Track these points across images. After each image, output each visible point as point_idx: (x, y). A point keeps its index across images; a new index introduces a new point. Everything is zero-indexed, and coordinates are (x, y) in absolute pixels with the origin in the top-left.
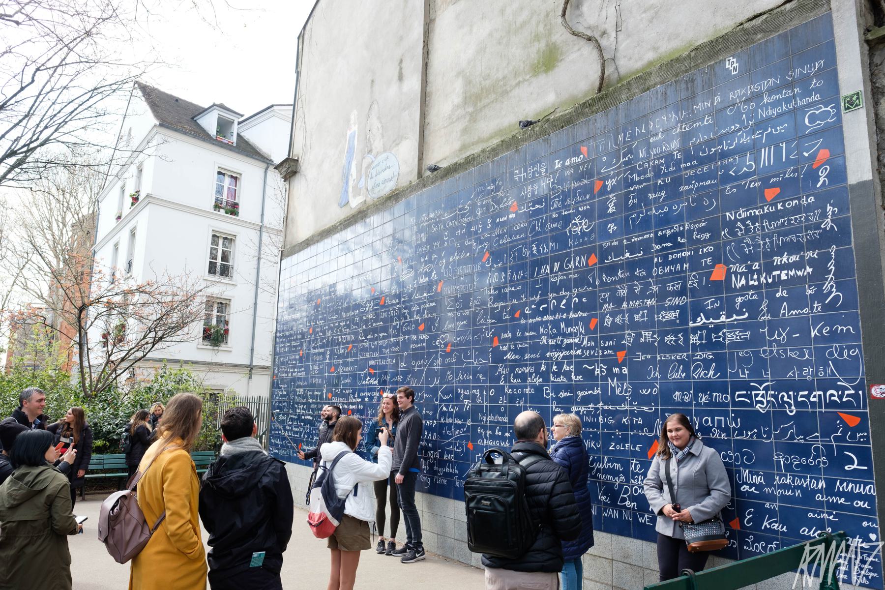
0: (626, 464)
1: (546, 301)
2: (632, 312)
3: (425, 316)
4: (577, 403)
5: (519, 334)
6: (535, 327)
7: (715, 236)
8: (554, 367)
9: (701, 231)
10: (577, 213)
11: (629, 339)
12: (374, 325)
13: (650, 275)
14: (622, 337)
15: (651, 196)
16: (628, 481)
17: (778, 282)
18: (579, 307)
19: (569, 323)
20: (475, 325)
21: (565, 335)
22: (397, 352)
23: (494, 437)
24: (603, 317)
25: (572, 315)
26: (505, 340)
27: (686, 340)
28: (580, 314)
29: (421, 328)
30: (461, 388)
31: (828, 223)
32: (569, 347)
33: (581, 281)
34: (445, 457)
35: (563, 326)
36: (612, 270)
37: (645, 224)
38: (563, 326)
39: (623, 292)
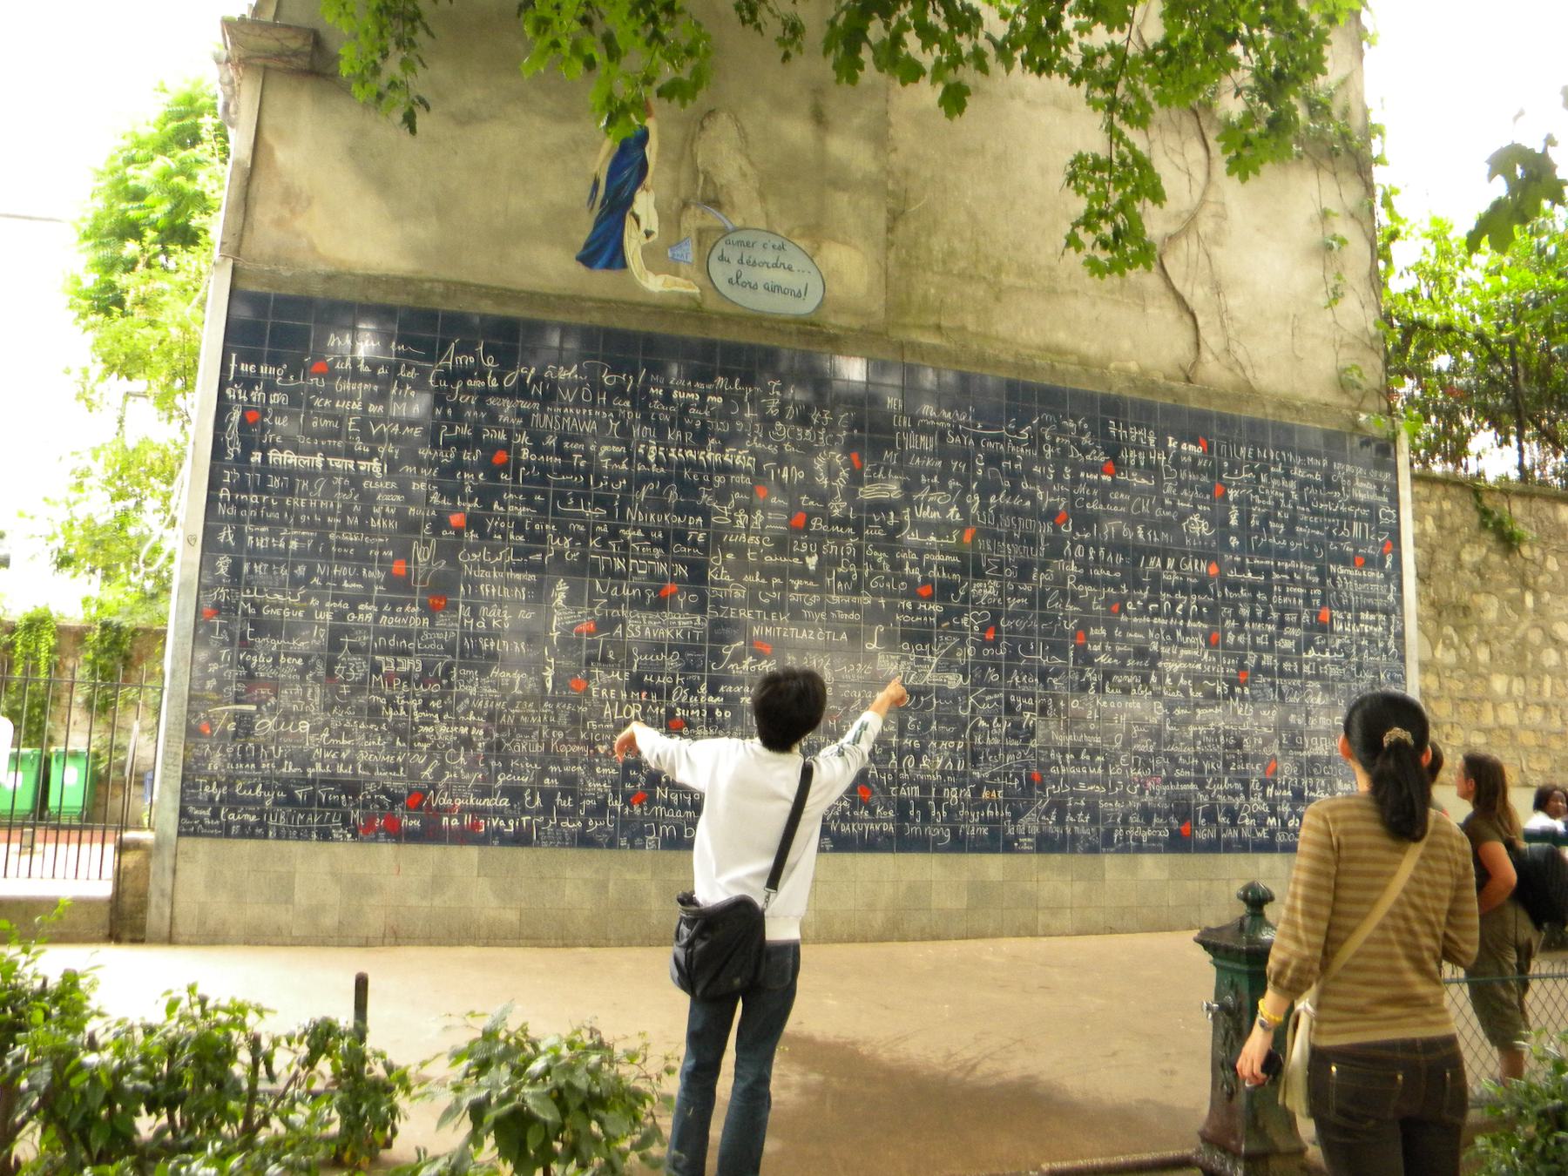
0: (1246, 784)
1: (1157, 601)
2: (1255, 634)
3: (934, 573)
4: (1196, 725)
5: (1118, 633)
6: (1143, 629)
7: (1322, 583)
8: (1168, 680)
9: (1312, 574)
10: (1195, 510)
11: (1251, 660)
12: (768, 559)
13: (1270, 601)
14: (1245, 657)
15: (1272, 525)
16: (1247, 798)
17: (1362, 634)
18: (1198, 617)
19: (1186, 632)
20: (1043, 606)
21: (1181, 645)
22: (853, 622)
23: (1077, 762)
24: (1225, 633)
25: (1189, 624)
26: (1096, 640)
27: (1300, 669)
28: (1200, 624)
29: (926, 591)
30: (1016, 694)
31: (1391, 598)
32: (1188, 660)
33: (1201, 588)
34: (985, 794)
35: (1179, 634)
36: (1235, 586)
37: (1266, 551)
38: (1179, 634)
39: (1245, 611)
